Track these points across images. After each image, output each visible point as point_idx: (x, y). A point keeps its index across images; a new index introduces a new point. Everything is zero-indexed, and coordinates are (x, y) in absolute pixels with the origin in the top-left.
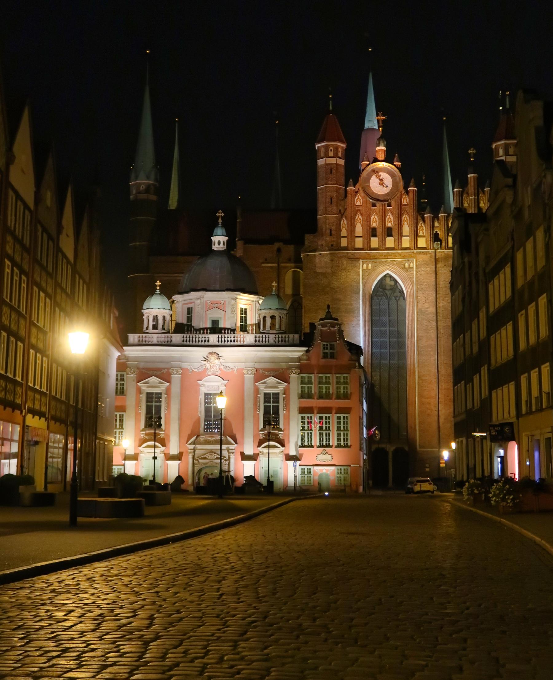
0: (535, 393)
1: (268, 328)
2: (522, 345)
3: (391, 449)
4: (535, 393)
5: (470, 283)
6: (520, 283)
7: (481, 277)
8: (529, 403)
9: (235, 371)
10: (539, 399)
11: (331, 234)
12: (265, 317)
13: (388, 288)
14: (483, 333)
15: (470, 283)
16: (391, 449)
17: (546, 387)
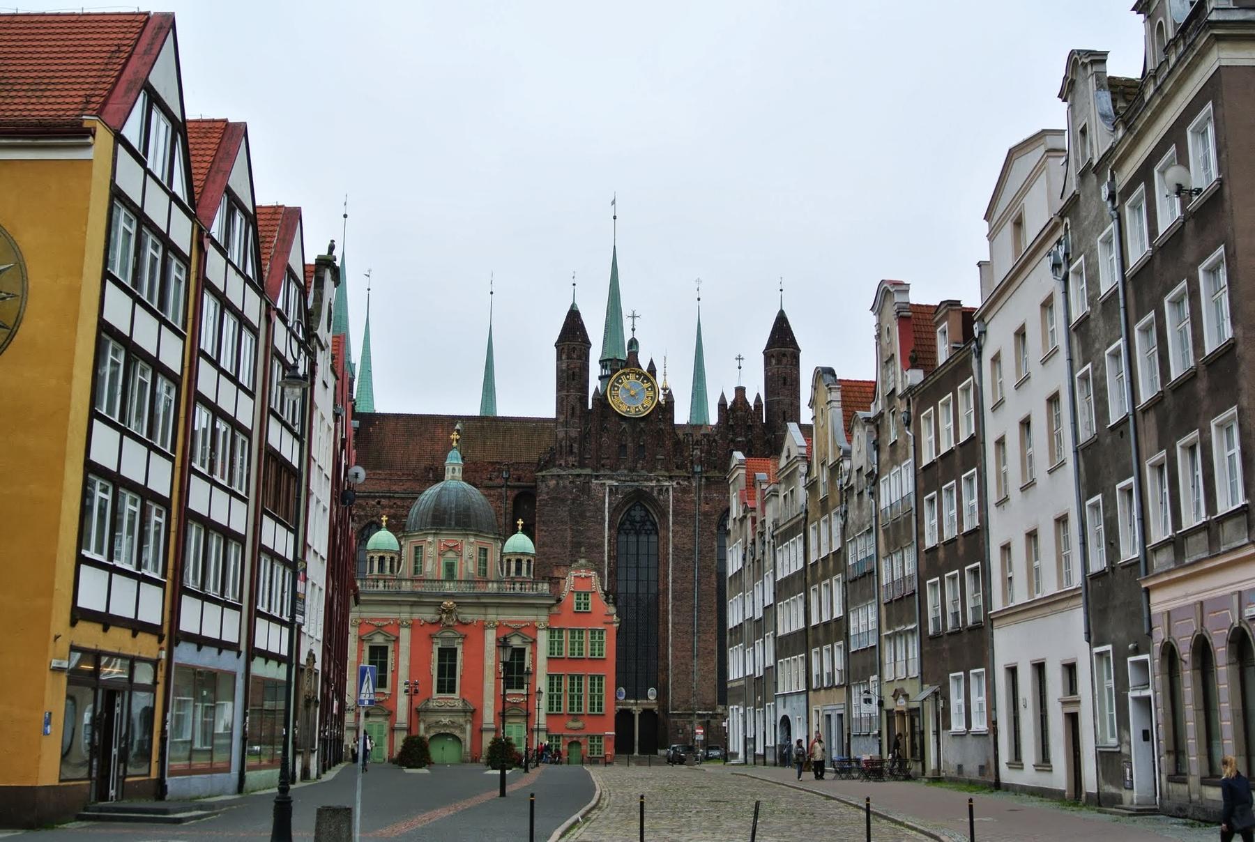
0: (827, 669)
1: (513, 574)
2: (815, 621)
3: (637, 711)
4: (827, 669)
5: (754, 543)
6: (813, 558)
7: (767, 537)
8: (820, 677)
10: (831, 676)
11: (571, 452)
12: (509, 561)
13: (638, 519)
14: (769, 600)
15: (754, 543)
16: (637, 711)
17: (839, 664)
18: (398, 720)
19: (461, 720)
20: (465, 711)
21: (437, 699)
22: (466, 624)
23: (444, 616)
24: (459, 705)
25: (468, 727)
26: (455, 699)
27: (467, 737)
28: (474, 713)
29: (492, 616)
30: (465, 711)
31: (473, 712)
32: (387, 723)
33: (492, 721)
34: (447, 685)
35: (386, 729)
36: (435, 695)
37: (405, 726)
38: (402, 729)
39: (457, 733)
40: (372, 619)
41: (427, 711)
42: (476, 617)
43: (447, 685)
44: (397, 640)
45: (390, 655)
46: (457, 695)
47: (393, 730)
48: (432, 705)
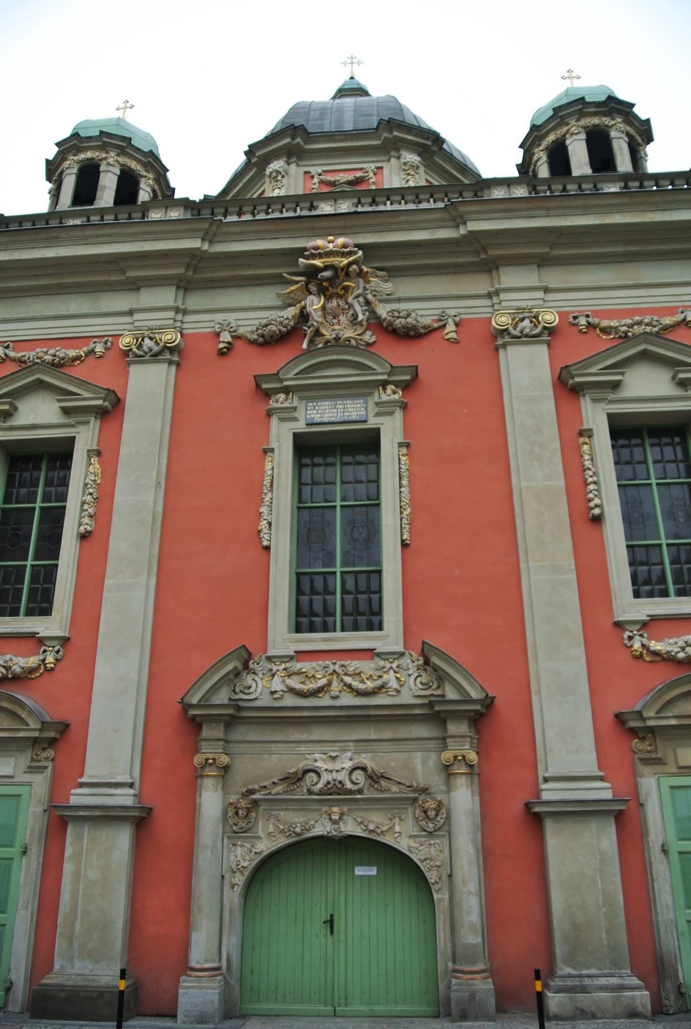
9: (451, 327)
18: (94, 769)
19: (418, 764)
20: (435, 714)
21: (287, 659)
22: (410, 334)
23: (314, 304)
24: (407, 686)
25: (463, 800)
26: (384, 660)
27: (459, 857)
28: (479, 720)
29: (523, 293)
30: (435, 714)
31: (481, 716)
32: (40, 783)
33: (586, 760)
34: (335, 597)
35: (30, 820)
36: (281, 637)
37: (124, 798)
38: (106, 817)
39: (403, 835)
40: (19, 343)
41: (236, 716)
42: (452, 308)
43: (335, 597)
44: (111, 410)
45: (81, 471)
46: (391, 635)
47: (59, 820)
48: (263, 687)
